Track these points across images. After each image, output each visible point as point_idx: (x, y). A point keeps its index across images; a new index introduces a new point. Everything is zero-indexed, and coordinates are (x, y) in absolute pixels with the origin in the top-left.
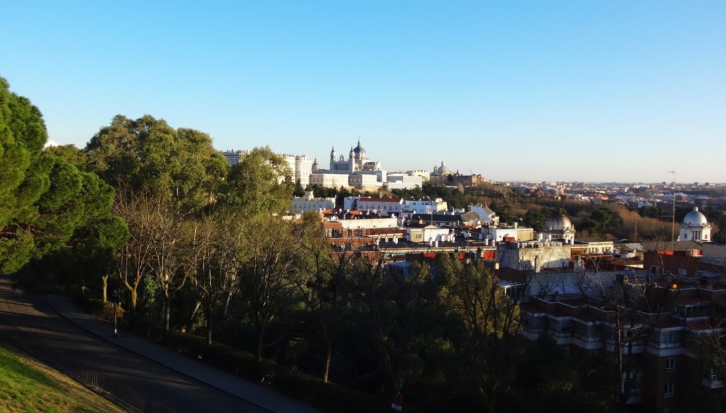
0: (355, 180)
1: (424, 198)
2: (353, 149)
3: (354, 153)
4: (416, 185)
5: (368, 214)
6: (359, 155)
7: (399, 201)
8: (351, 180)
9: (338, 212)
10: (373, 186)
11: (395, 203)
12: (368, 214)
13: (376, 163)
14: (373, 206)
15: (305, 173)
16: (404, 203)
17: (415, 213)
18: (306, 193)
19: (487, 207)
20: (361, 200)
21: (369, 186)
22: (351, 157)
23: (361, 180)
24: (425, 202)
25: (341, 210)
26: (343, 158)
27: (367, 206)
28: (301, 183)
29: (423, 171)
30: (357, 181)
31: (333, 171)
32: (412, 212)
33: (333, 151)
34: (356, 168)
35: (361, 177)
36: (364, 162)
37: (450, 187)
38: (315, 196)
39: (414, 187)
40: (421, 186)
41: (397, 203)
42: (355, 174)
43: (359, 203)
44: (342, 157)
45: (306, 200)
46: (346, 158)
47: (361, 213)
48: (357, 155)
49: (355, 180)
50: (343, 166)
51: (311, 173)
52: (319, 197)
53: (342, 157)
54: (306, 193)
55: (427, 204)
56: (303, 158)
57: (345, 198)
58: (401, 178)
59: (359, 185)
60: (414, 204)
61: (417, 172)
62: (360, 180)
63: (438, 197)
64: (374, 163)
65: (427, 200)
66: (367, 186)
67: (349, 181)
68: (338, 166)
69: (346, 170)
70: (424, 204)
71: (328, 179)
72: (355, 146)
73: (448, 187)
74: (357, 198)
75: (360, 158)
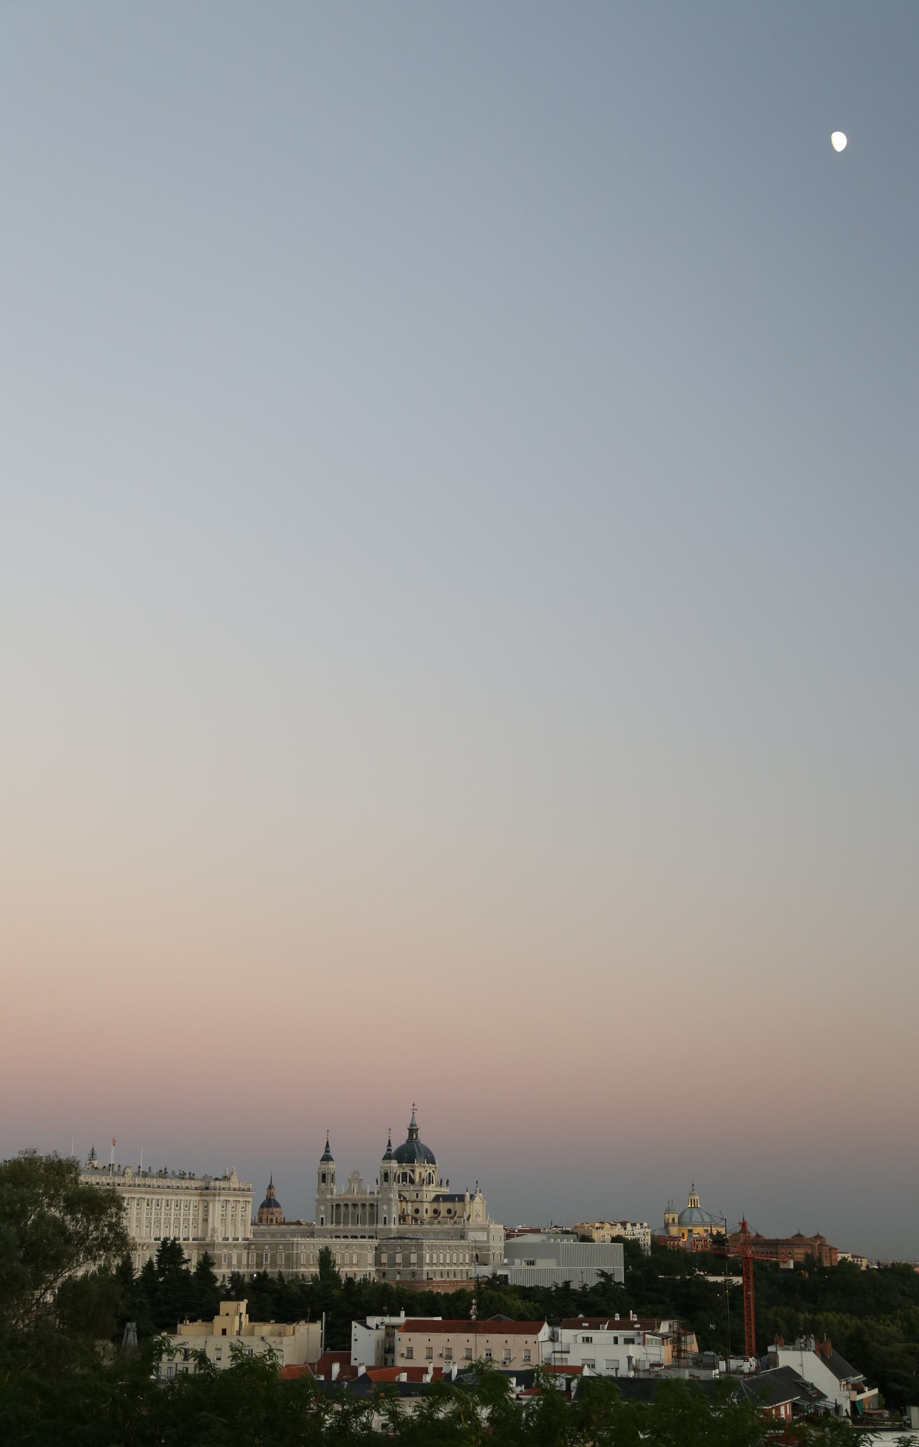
0: (399, 1258)
1: (617, 1318)
2: (394, 1148)
4: (603, 1274)
5: (427, 1379)
6: (413, 1171)
7: (536, 1331)
8: (384, 1258)
9: (329, 1373)
11: (522, 1338)
12: (427, 1379)
13: (468, 1198)
14: (449, 1349)
15: (230, 1236)
16: (553, 1339)
17: (586, 1372)
18: (225, 1306)
19: (831, 1352)
20: (409, 1327)
21: (452, 1278)
23: (421, 1258)
24: (622, 1334)
25: (336, 1368)
27: (430, 1349)
28: (215, 1271)
29: (629, 1226)
30: (407, 1262)
32: (581, 1369)
34: (403, 1218)
35: (420, 1247)
36: (431, 1191)
37: (720, 1279)
38: (257, 1315)
39: (593, 1281)
40: (620, 1277)
41: (530, 1338)
43: (403, 1340)
44: (356, 1178)
45: (224, 1332)
47: (404, 1377)
48: (407, 1170)
49: (399, 1258)
50: (359, 1210)
51: (250, 1236)
52: (265, 1320)
53: (356, 1178)
54: (225, 1306)
55: (629, 1341)
57: (354, 1324)
58: (550, 1251)
59: (414, 1274)
60: (588, 1340)
61: (607, 1226)
62: (414, 1258)
63: (665, 1318)
64: (461, 1198)
65: (630, 1326)
66: (438, 1278)
67: (378, 1262)
68: (342, 1209)
69: (372, 1223)
70: (621, 1340)
72: (400, 1139)
73: (712, 1279)
74: (394, 1320)
75: (417, 1179)
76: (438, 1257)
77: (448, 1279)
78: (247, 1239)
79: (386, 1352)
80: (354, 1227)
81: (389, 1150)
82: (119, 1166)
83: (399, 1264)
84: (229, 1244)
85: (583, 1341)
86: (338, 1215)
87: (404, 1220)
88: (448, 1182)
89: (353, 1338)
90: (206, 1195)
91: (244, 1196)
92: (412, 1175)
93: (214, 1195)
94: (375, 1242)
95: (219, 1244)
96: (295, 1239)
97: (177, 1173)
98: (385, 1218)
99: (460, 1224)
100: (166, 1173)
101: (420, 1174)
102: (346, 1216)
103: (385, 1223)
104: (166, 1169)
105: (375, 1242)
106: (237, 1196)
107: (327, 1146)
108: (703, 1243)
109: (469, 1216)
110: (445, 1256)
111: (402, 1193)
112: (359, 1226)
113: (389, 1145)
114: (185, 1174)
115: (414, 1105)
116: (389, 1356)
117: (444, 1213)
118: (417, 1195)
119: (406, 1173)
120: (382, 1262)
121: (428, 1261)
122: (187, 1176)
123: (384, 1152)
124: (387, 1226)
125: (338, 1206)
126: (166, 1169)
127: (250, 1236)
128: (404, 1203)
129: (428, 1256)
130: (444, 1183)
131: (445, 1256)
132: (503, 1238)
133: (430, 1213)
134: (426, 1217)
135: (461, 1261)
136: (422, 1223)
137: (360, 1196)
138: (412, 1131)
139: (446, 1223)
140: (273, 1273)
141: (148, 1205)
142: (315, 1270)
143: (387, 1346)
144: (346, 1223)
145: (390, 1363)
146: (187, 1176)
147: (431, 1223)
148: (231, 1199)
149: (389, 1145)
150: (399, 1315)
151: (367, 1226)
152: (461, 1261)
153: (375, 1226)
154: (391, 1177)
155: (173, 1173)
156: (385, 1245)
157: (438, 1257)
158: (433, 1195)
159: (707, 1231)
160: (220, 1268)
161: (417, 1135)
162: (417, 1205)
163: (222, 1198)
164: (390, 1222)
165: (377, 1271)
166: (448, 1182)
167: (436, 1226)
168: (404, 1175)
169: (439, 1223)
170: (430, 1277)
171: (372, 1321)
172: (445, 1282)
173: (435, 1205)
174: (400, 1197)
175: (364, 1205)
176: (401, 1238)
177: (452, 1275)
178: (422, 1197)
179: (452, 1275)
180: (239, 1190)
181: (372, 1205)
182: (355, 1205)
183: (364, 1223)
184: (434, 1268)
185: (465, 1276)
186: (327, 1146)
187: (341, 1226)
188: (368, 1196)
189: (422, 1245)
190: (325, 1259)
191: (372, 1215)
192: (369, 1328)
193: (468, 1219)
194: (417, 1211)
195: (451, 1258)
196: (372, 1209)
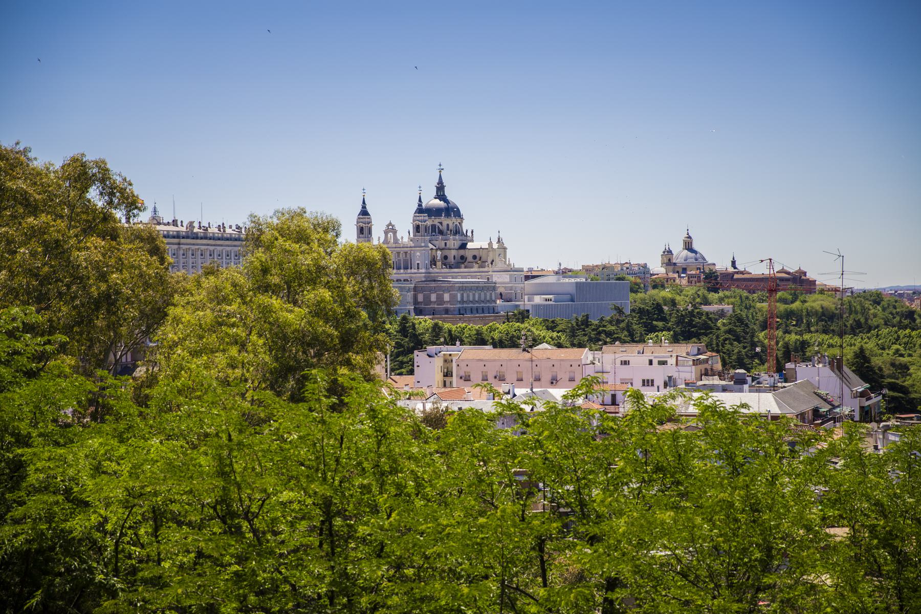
6: (441, 223)
8: (420, 298)
22: (417, 229)
26: (395, 232)
30: (440, 300)
33: (364, 213)
44: (391, 229)
46: (405, 232)
49: (433, 297)
53: (391, 229)
60: (625, 363)
67: (416, 302)
69: (406, 268)
70: (655, 362)
76: (468, 296)
79: (444, 376)
82: (182, 222)
83: (435, 302)
85: (622, 364)
87: (435, 265)
88: (472, 232)
89: (416, 365)
92: (440, 226)
97: (234, 228)
98: (418, 264)
100: (224, 227)
103: (418, 268)
104: (223, 224)
107: (364, 202)
108: (696, 279)
109: (493, 261)
110: (474, 295)
113: (420, 200)
115: (440, 165)
116: (448, 379)
118: (446, 244)
119: (435, 225)
120: (419, 300)
121: (459, 299)
123: (416, 207)
126: (223, 224)
130: (469, 234)
131: (474, 295)
133: (458, 258)
135: (488, 298)
136: (451, 267)
137: (394, 246)
138: (440, 188)
141: (210, 255)
143: (446, 370)
145: (448, 384)
147: (459, 267)
149: (420, 200)
150: (455, 345)
151: (402, 271)
152: (488, 298)
153: (409, 271)
154: (422, 229)
157: (468, 296)
159: (700, 269)
162: (446, 252)
165: (415, 309)
166: (472, 232)
168: (433, 226)
169: (465, 267)
170: (462, 312)
171: (432, 349)
176: (435, 281)
177: (480, 311)
181: (406, 253)
183: (399, 268)
186: (364, 202)
188: (402, 246)
191: (406, 262)
192: (430, 356)
193: (492, 264)
194: (446, 257)
195: (480, 297)
196: (406, 256)
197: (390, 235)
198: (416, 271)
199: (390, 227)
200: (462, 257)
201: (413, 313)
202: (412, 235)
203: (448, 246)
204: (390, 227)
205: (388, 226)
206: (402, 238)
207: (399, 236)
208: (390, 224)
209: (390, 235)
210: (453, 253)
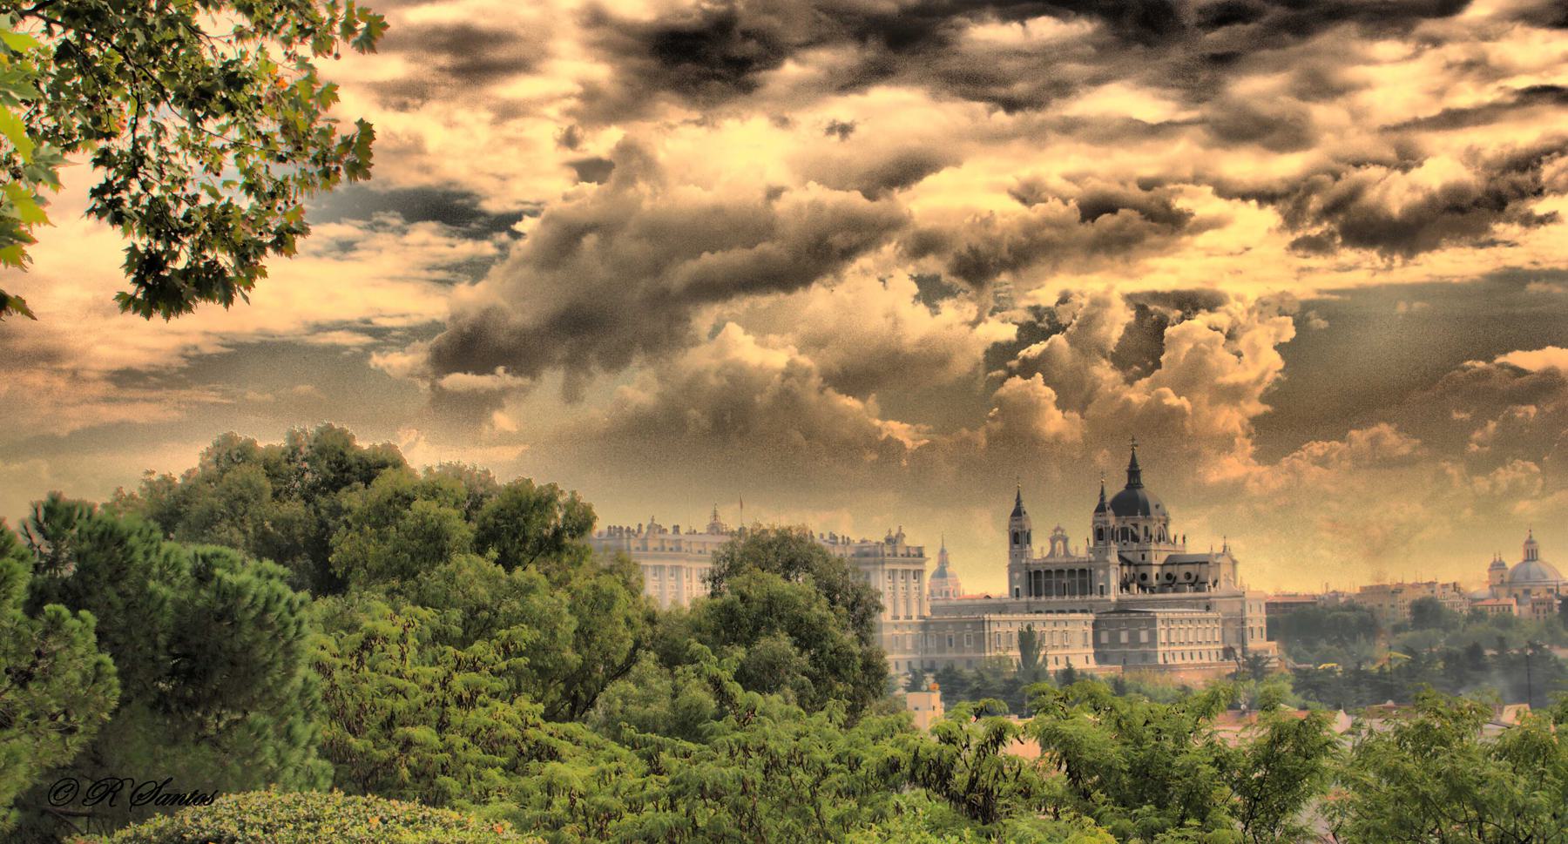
0: (1124, 638)
2: (1109, 499)
3: (1112, 520)
6: (1136, 526)
8: (1104, 638)
10: (1205, 660)
15: (902, 613)
21: (1196, 660)
22: (1099, 534)
23: (1153, 636)
26: (1065, 541)
31: (1024, 599)
34: (1125, 585)
36: (1158, 555)
42: (1122, 608)
48: (1129, 525)
49: (1124, 638)
50: (1065, 580)
51: (927, 613)
56: (887, 550)
62: (1144, 636)
66: (1179, 661)
67: (1097, 643)
69: (1083, 593)
71: (1002, 629)
77: (1192, 662)
78: (924, 617)
80: (1060, 599)
81: (1102, 499)
83: (1125, 644)
84: (902, 624)
86: (1038, 586)
87: (1128, 589)
90: (867, 564)
91: (915, 563)
93: (875, 563)
94: (1091, 617)
95: (887, 624)
96: (986, 616)
97: (827, 537)
99: (1204, 591)
101: (1146, 528)
102: (1048, 586)
103: (1102, 593)
105: (1091, 617)
106: (907, 563)
107: (1018, 501)
111: (1124, 555)
112: (1067, 598)
114: (836, 538)
117: (1181, 578)
118: (1143, 557)
122: (840, 540)
124: (1105, 597)
125: (1037, 573)
127: (927, 613)
128: (1125, 569)
129: (1163, 633)
130: (1179, 541)
132: (1263, 608)
134: (1155, 582)
136: (1152, 591)
137: (1065, 560)
139: (1185, 591)
140: (960, 658)
142: (1015, 654)
144: (1048, 594)
146: (840, 540)
147: (1162, 591)
148: (900, 567)
151: (1077, 598)
153: (1088, 597)
154: (1107, 534)
155: (822, 536)
156: (1106, 621)
158: (1163, 557)
160: (892, 651)
161: (1139, 478)
162: (1143, 570)
163: (887, 567)
164: (1108, 592)
165: (1096, 654)
167: (1170, 595)
168: (1125, 532)
169: (1175, 591)
172: (1188, 665)
173: (1169, 569)
174: (1121, 557)
175: (1072, 572)
177: (1196, 656)
178: (1151, 558)
179: (1196, 656)
180: (909, 555)
181: (1083, 571)
182: (1060, 572)
184: (1172, 648)
185: (1214, 659)
187: (1043, 598)
189: (1154, 620)
190: (1028, 642)
193: (1214, 585)
194: (1144, 577)
197: (1059, 544)
198: (1098, 597)
199: (1059, 533)
200: (1169, 576)
201: (1091, 658)
202: (1091, 545)
203: (1146, 560)
204: (1059, 533)
205: (1056, 530)
206: (1077, 549)
207: (1071, 546)
208: (1058, 529)
209: (1059, 544)
210: (1156, 570)
